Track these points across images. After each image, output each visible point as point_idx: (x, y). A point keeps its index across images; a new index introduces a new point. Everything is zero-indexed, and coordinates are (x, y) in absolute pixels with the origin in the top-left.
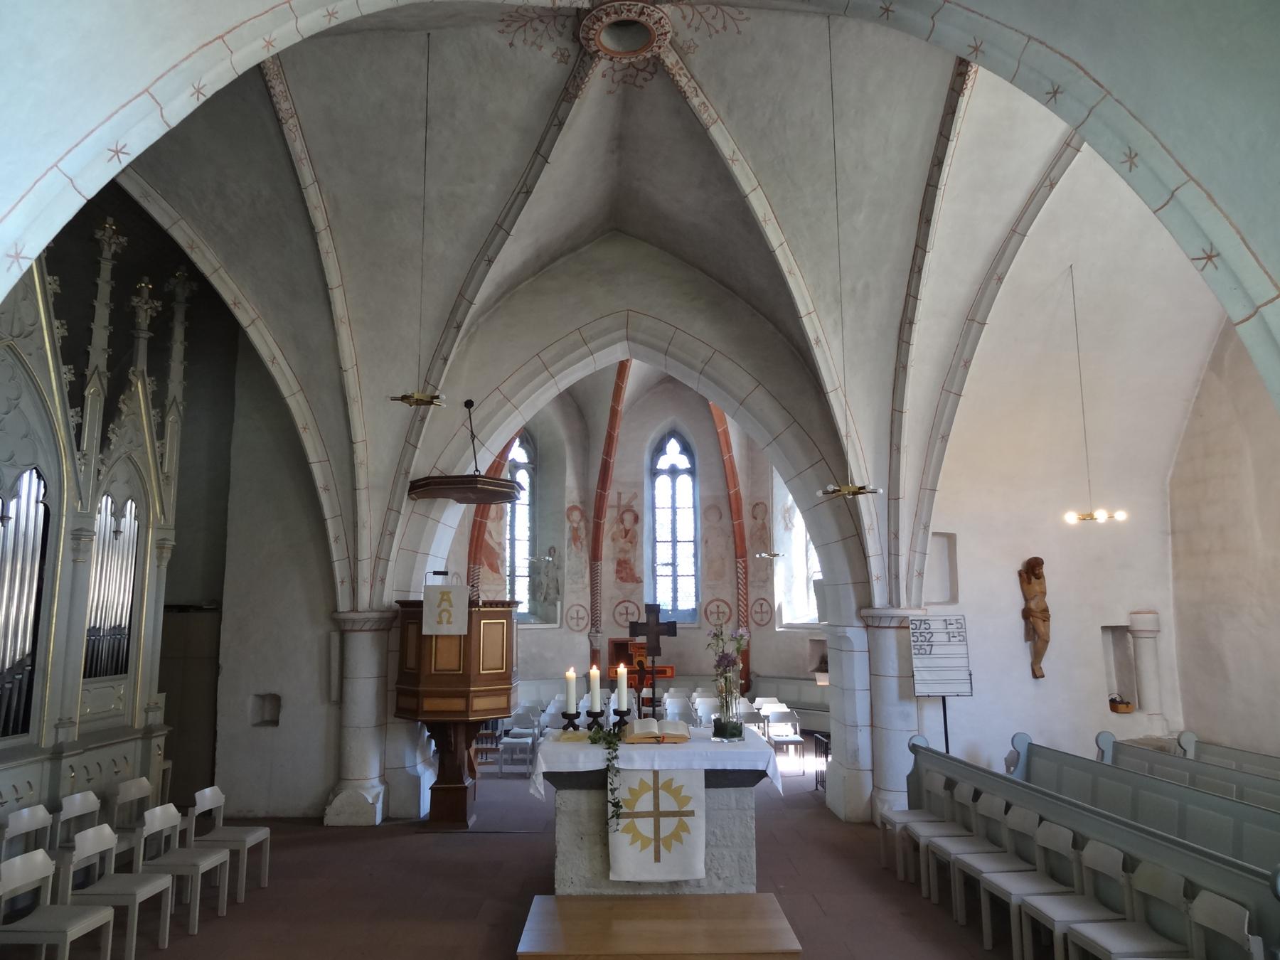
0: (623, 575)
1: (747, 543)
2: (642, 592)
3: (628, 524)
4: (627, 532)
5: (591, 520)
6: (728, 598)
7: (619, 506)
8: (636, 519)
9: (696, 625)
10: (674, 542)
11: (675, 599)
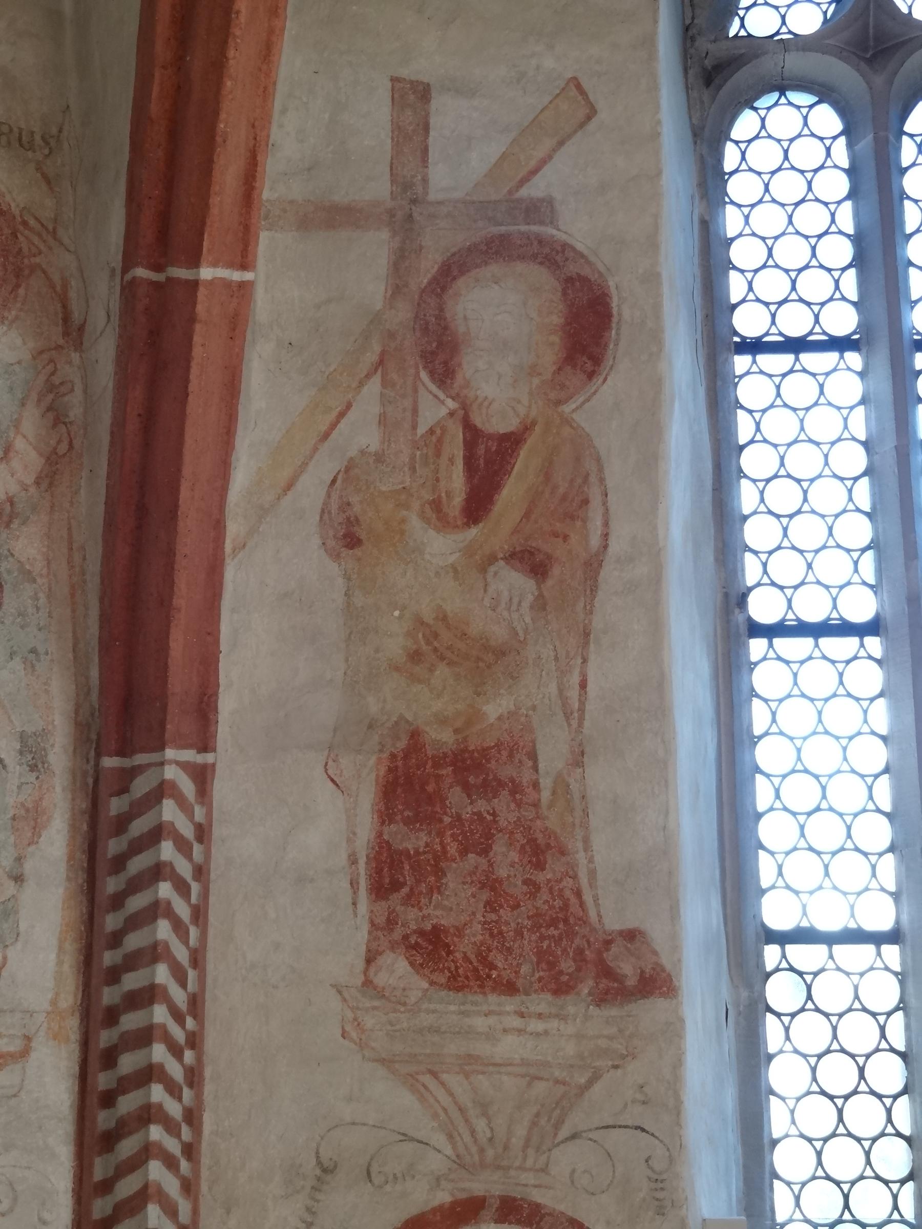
0: (456, 904)
2: (665, 1100)
3: (499, 386)
4: (488, 460)
5: (101, 307)
7: (405, 213)
8: (588, 329)
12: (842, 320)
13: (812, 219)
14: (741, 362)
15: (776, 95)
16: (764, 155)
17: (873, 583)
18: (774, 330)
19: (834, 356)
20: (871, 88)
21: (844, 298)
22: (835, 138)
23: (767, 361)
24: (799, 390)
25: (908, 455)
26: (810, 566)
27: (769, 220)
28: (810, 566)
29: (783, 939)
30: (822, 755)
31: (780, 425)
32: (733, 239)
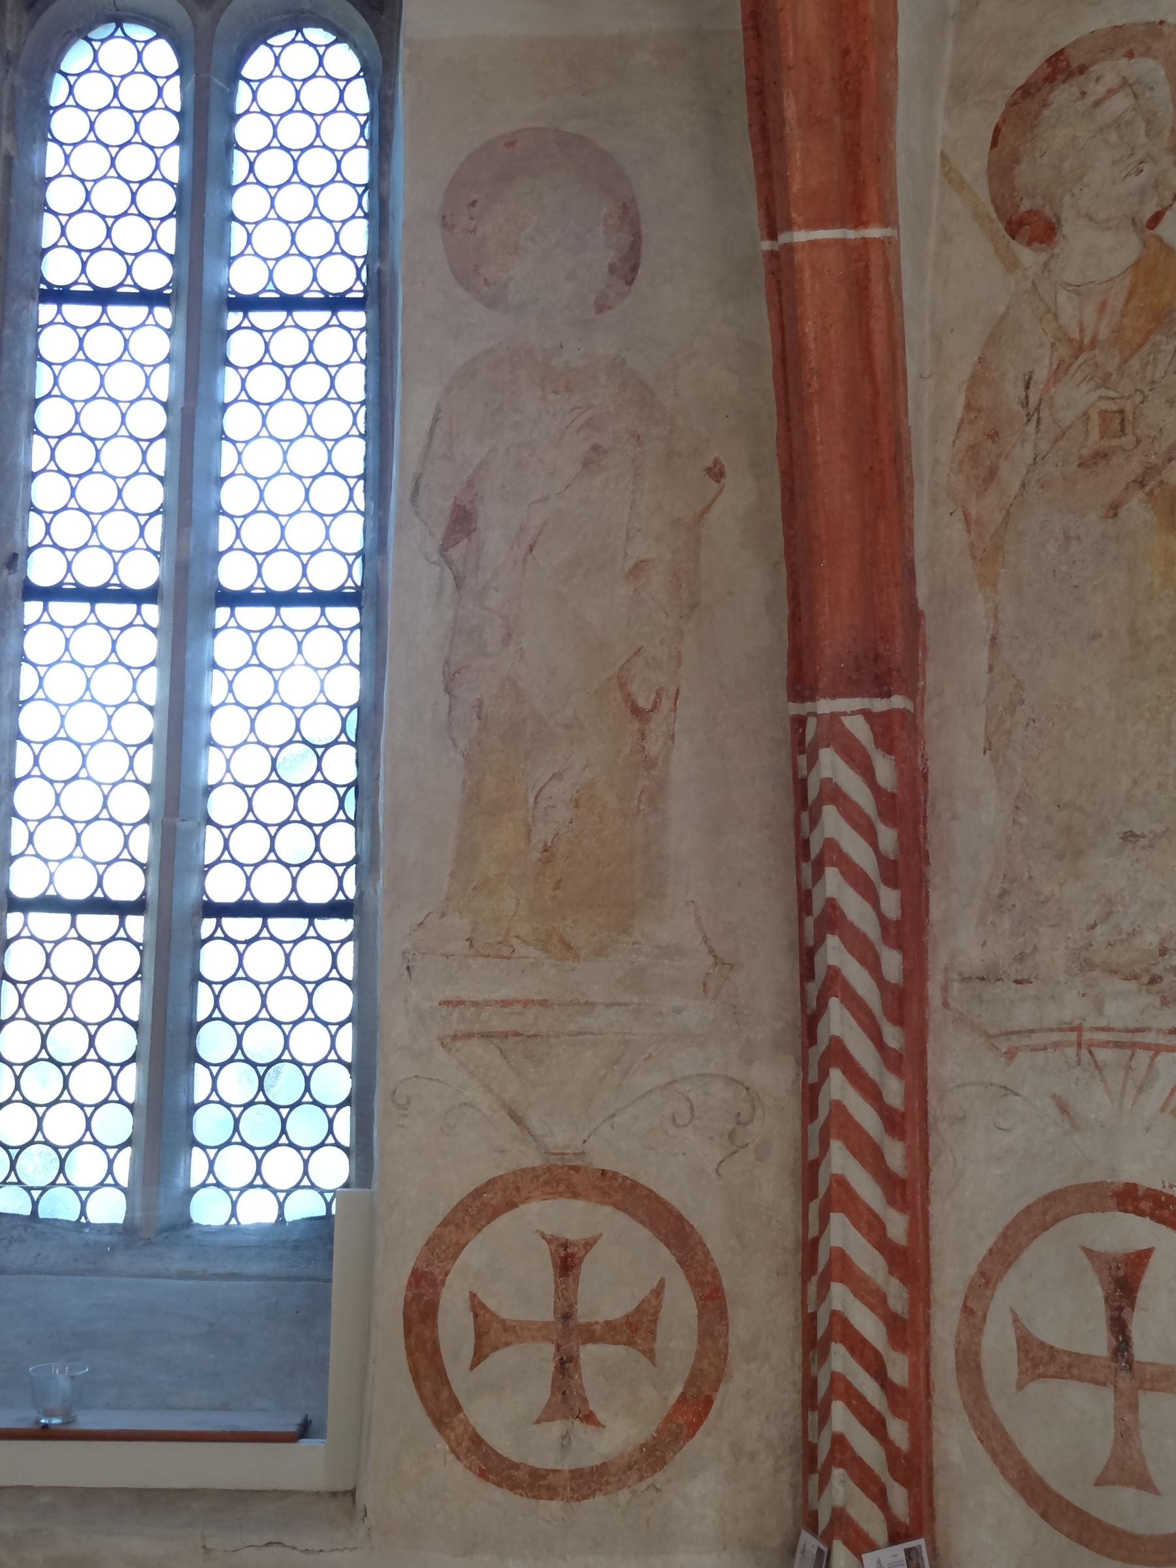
1: (937, 533)
6: (677, 1172)
9: (304, 1466)
10: (189, 598)
11: (163, 1127)
12: (156, 273)
13: (135, 163)
14: (46, 311)
15: (113, 26)
16: (94, 91)
17: (158, 550)
18: (83, 279)
19: (143, 310)
20: (195, 25)
21: (160, 250)
22: (168, 78)
23: (73, 312)
24: (104, 344)
25: (194, 418)
26: (94, 529)
27: (91, 161)
28: (94, 529)
29: (26, 906)
30: (86, 723)
31: (79, 382)
32: (50, 179)
